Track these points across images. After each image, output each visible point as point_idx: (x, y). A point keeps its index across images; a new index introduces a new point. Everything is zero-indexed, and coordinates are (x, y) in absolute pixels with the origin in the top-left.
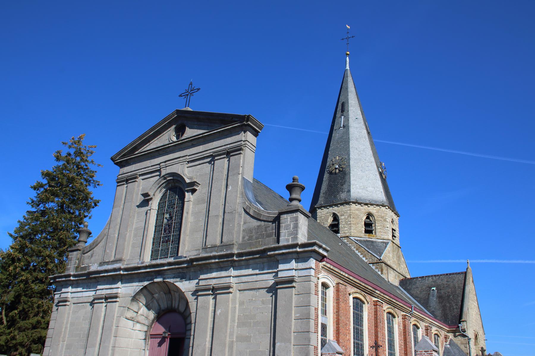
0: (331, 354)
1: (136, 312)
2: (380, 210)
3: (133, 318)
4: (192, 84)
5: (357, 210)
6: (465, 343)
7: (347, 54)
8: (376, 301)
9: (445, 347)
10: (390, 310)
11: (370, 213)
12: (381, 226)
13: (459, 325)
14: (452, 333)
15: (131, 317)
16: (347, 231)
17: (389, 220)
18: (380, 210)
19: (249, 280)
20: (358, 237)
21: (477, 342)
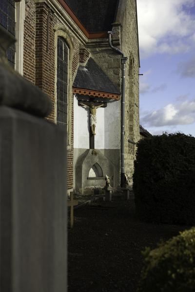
6: (116, 65)
13: (109, 32)
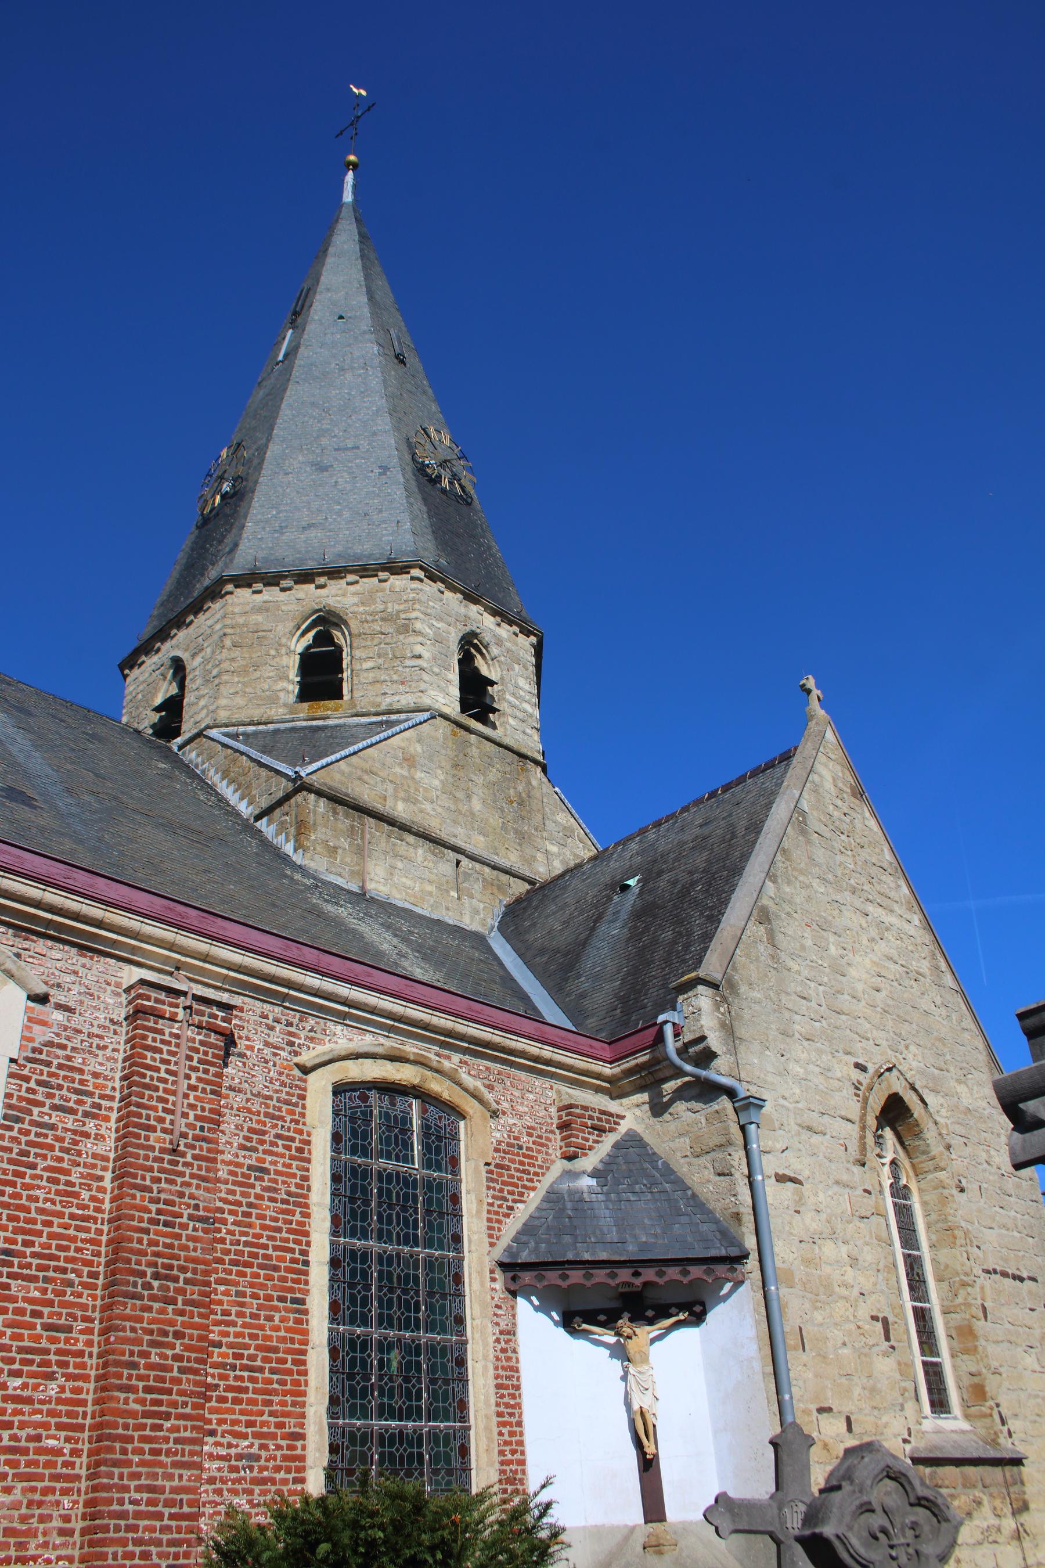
2: (383, 590)
6: (717, 1140)
7: (350, 163)
9: (553, 1197)
11: (331, 613)
14: (641, 1089)
18: (383, 590)
21: (924, 1153)
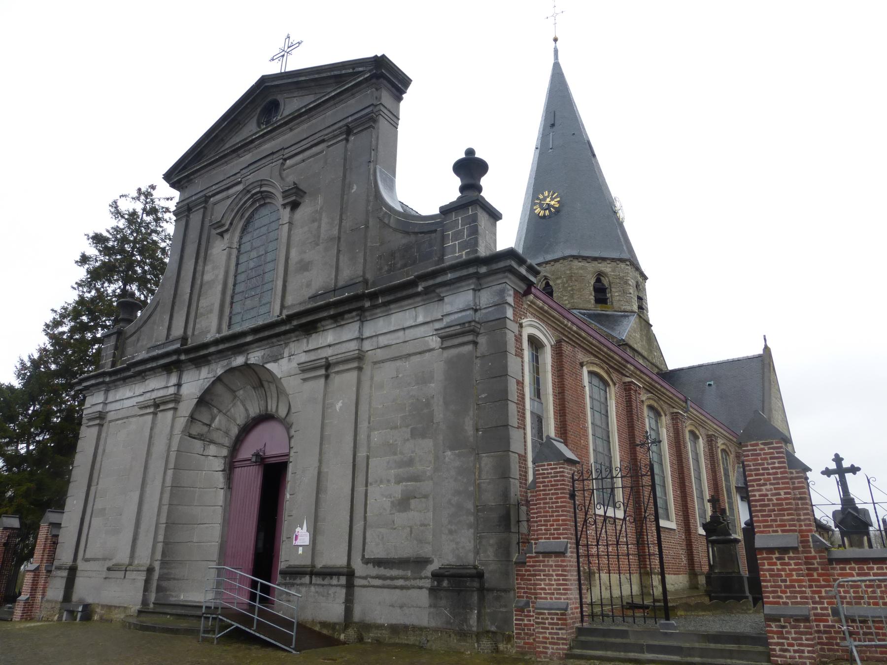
0: (554, 465)
1: (207, 425)
3: (202, 435)
4: (289, 37)
5: (581, 268)
8: (629, 382)
10: (652, 402)
11: (602, 273)
12: (620, 291)
15: (198, 435)
16: (567, 302)
17: (632, 282)
18: (618, 267)
19: (391, 342)
20: (585, 310)
